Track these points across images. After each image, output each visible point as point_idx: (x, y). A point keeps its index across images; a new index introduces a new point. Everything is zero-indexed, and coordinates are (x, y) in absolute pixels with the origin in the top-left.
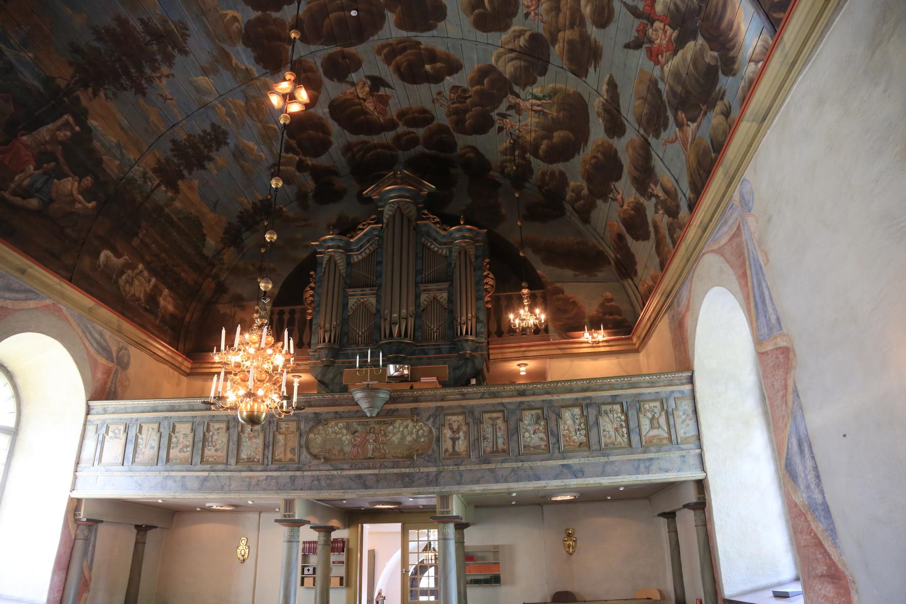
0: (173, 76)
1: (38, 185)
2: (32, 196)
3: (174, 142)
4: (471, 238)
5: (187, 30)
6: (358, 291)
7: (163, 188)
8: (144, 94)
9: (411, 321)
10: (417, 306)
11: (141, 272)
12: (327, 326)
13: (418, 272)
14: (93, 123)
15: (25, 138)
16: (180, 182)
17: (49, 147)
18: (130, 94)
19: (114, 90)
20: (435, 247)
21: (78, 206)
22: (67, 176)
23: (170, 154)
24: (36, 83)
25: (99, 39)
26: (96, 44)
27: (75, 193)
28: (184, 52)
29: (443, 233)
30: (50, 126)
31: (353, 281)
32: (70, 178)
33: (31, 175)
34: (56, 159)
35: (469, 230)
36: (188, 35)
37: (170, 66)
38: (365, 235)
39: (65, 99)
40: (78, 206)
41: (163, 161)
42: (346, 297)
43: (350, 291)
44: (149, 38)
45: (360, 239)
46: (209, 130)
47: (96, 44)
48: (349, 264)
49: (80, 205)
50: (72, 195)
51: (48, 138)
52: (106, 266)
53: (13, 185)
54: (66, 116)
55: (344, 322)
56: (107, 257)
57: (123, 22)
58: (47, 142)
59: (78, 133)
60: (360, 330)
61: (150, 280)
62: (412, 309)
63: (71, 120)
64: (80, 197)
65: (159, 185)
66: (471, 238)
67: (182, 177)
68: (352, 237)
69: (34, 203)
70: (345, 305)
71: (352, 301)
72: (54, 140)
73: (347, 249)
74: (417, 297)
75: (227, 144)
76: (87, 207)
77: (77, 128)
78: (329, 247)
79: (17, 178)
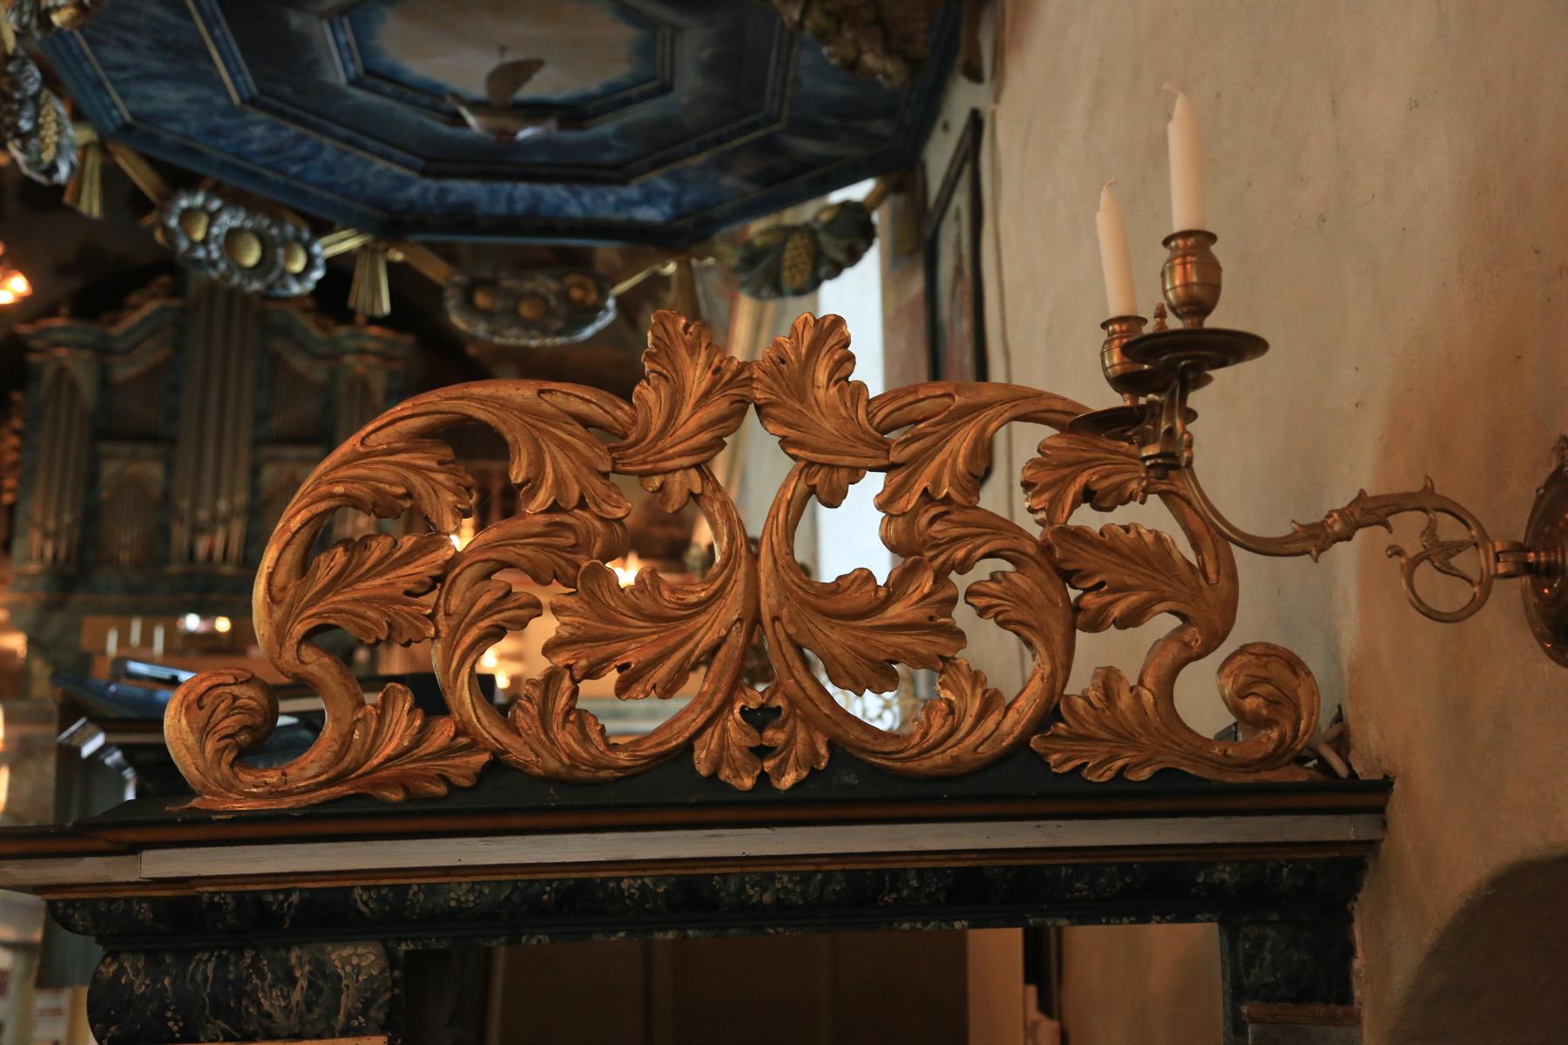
4: (377, 354)
6: (126, 449)
9: (237, 527)
10: (254, 491)
12: (51, 524)
13: (260, 417)
20: (299, 363)
29: (316, 333)
31: (110, 427)
35: (378, 339)
38: (145, 321)
42: (95, 461)
43: (106, 448)
45: (131, 331)
48: (104, 383)
55: (91, 516)
60: (125, 539)
62: (241, 499)
66: (377, 354)
68: (113, 323)
70: (92, 478)
71: (109, 469)
73: (103, 351)
74: (255, 472)
78: (58, 344)
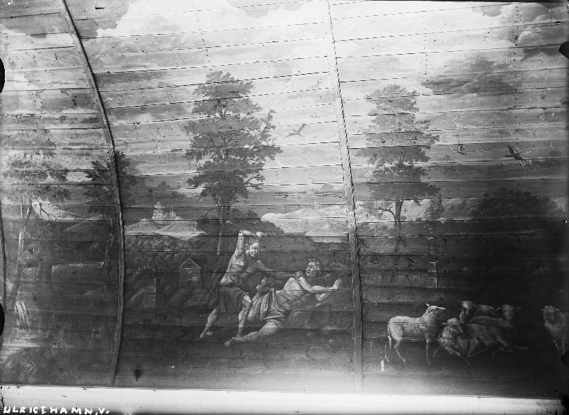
0: (272, 111)
1: (264, 309)
2: (265, 322)
3: (363, 152)
5: (221, 72)
7: (408, 204)
8: (278, 150)
11: (472, 311)
14: (267, 217)
15: (223, 280)
16: (423, 179)
17: (249, 270)
18: (268, 164)
19: (255, 175)
21: (320, 297)
22: (286, 280)
23: (373, 166)
24: (197, 233)
25: (199, 156)
26: (202, 162)
27: (307, 287)
28: (247, 87)
30: (236, 252)
32: (291, 279)
33: (251, 305)
34: (264, 274)
36: (228, 75)
37: (259, 109)
39: (227, 222)
40: (320, 297)
41: (375, 180)
44: (217, 115)
46: (374, 106)
47: (202, 162)
49: (323, 295)
50: (306, 292)
51: (242, 264)
52: (405, 335)
53: (241, 326)
54: (240, 234)
56: (401, 325)
57: (191, 127)
58: (244, 268)
59: (263, 237)
61: (501, 314)
63: (247, 233)
64: (317, 288)
65: (399, 205)
67: (419, 171)
69: (270, 326)
72: (248, 260)
75: (414, 94)
76: (334, 291)
77: (259, 234)
79: (240, 317)
